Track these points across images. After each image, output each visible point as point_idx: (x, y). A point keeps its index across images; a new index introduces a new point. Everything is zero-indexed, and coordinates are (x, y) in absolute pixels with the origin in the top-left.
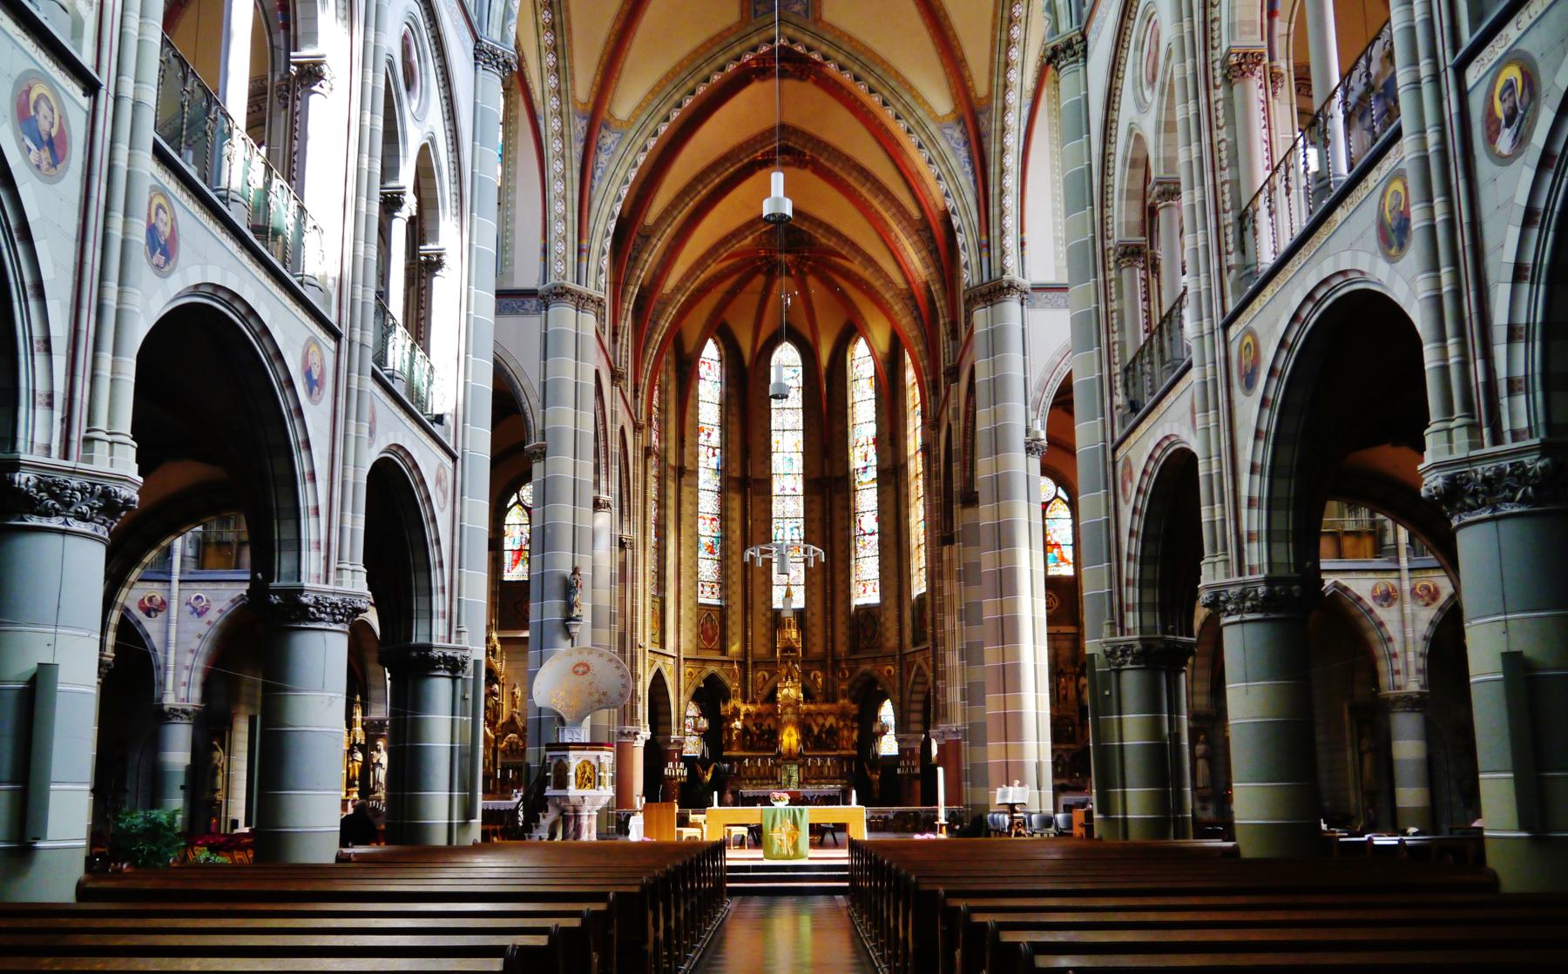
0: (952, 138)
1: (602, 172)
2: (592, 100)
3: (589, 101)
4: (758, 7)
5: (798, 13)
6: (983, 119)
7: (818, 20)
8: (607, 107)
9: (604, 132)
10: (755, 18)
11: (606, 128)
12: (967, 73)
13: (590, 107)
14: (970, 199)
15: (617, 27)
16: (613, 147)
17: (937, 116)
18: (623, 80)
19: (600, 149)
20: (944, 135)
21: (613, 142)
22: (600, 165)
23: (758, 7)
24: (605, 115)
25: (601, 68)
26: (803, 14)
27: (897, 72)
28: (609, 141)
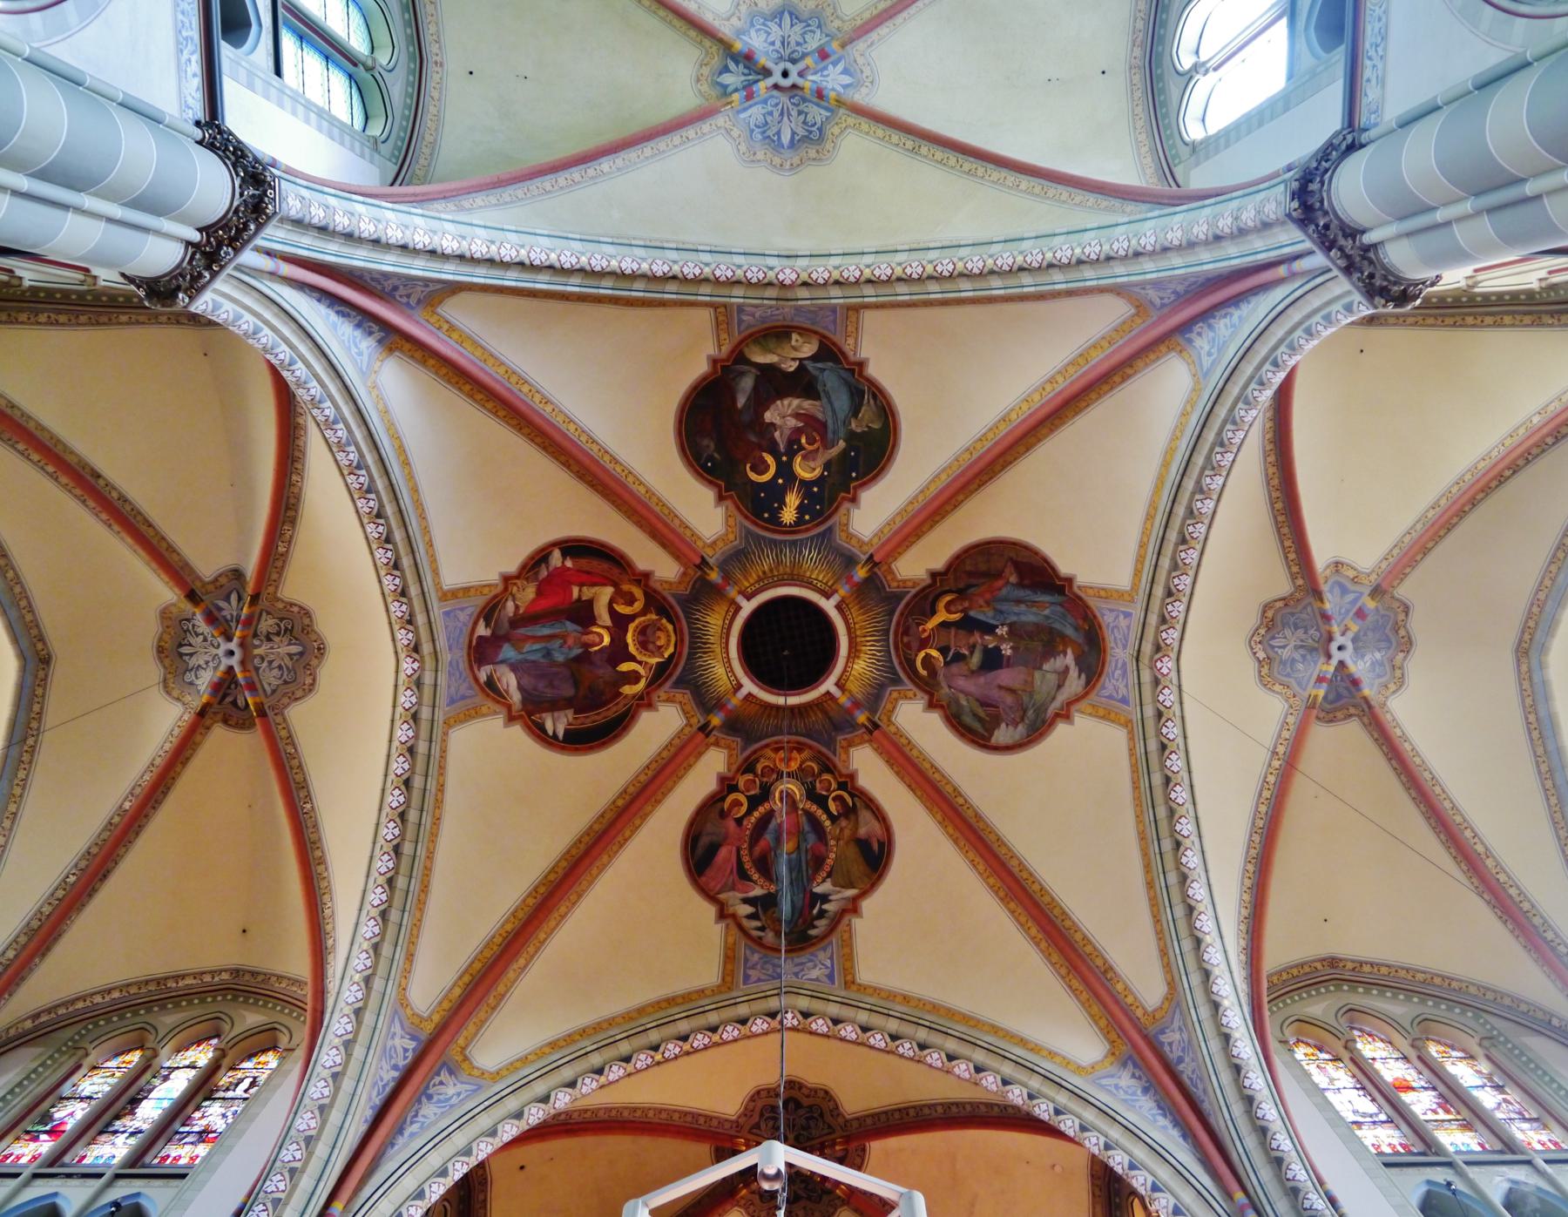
0: (1117, 1087)
1: (421, 1128)
2: (436, 1018)
3: (430, 1018)
4: (750, 972)
5: (817, 980)
6: (1172, 1039)
7: (850, 983)
8: (461, 1041)
9: (444, 1076)
10: (745, 984)
11: (451, 1072)
12: (1119, 987)
13: (429, 1028)
14: (1184, 1155)
15: (509, 927)
16: (454, 1101)
17: (1079, 1067)
18: (508, 1007)
19: (430, 1097)
20: (1102, 1087)
21: (459, 1094)
22: (420, 1119)
23: (750, 972)
24: (454, 1053)
25: (467, 979)
26: (826, 979)
27: (993, 1026)
28: (451, 1091)
